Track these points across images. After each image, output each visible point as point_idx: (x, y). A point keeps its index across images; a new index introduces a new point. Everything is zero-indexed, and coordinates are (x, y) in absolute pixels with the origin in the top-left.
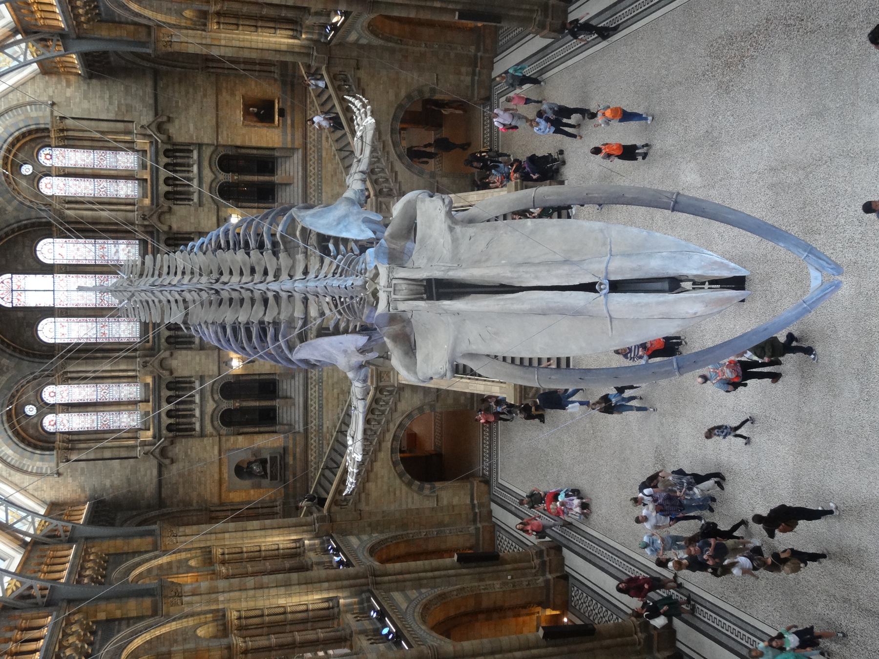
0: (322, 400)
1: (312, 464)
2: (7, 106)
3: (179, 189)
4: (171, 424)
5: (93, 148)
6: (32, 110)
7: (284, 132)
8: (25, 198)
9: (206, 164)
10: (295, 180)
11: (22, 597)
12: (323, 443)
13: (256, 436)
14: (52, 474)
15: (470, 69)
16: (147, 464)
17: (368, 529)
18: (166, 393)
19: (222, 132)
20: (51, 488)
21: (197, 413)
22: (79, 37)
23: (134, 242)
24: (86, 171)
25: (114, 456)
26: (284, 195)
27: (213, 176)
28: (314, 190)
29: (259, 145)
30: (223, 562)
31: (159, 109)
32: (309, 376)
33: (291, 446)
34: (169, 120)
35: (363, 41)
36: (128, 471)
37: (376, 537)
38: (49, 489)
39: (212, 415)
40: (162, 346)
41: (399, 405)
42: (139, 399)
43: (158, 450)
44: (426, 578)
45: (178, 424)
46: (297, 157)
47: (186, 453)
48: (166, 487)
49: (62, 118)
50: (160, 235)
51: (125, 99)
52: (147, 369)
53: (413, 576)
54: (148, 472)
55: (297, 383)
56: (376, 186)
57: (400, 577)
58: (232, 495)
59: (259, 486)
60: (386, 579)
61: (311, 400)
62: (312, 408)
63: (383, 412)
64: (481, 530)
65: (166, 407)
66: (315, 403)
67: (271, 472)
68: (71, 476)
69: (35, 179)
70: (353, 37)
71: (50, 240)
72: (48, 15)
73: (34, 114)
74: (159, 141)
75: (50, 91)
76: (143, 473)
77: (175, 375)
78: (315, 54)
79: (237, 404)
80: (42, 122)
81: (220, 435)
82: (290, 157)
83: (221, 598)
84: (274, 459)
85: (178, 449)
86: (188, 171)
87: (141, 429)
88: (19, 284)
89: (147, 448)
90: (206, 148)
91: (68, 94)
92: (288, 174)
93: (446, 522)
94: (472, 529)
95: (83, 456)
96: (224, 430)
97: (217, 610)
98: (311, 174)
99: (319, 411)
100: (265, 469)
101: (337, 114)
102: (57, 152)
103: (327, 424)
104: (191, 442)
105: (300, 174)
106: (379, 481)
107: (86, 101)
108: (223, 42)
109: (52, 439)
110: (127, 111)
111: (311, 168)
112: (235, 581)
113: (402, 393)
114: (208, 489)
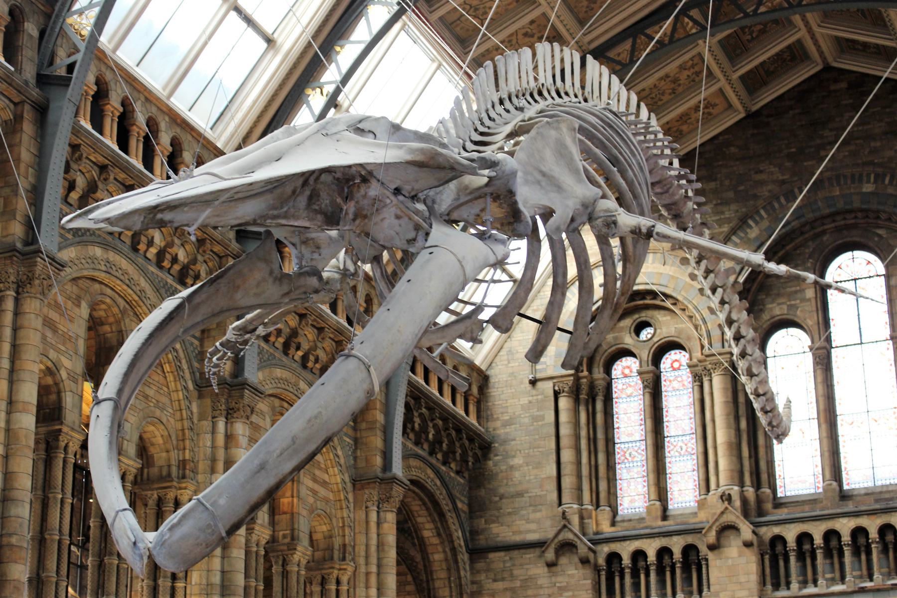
16: (548, 523)
18: (677, 545)
20: (512, 375)
25: (562, 466)
36: (537, 492)
40: (763, 530)
42: (670, 507)
43: (570, 536)
48: (507, 558)
54: (533, 526)
65: (651, 548)
68: (530, 402)
76: (532, 516)
77: (711, 556)
87: (615, 513)
89: (575, 520)
95: (564, 417)
97: (195, 471)
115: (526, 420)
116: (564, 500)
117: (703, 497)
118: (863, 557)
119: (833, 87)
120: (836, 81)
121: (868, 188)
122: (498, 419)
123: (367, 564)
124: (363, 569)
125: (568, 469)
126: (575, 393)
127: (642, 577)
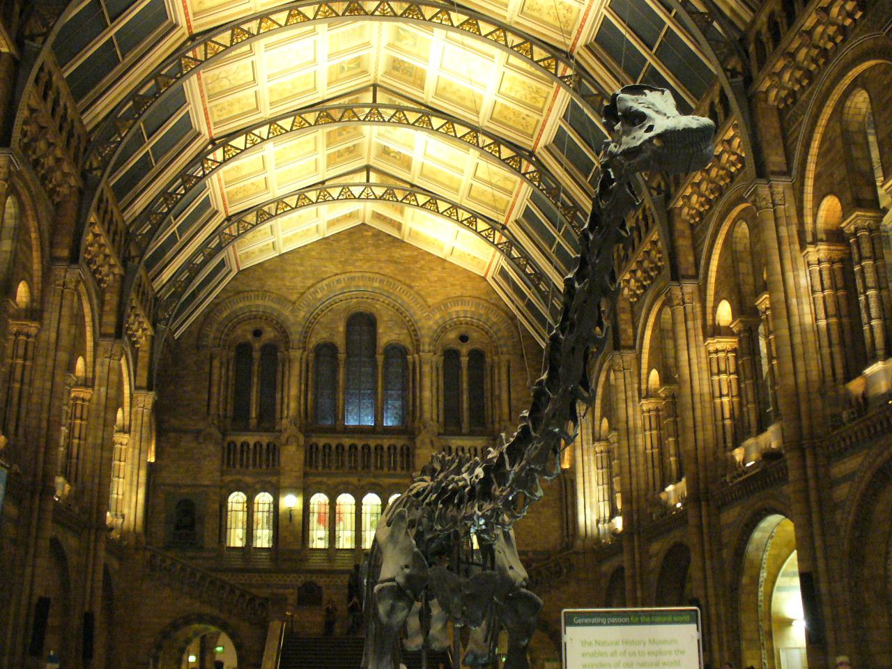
47: (205, 456)
83: (103, 389)
89: (216, 422)
95: (216, 372)
108: (586, 458)
119: (365, 233)
120: (367, 231)
121: (376, 285)
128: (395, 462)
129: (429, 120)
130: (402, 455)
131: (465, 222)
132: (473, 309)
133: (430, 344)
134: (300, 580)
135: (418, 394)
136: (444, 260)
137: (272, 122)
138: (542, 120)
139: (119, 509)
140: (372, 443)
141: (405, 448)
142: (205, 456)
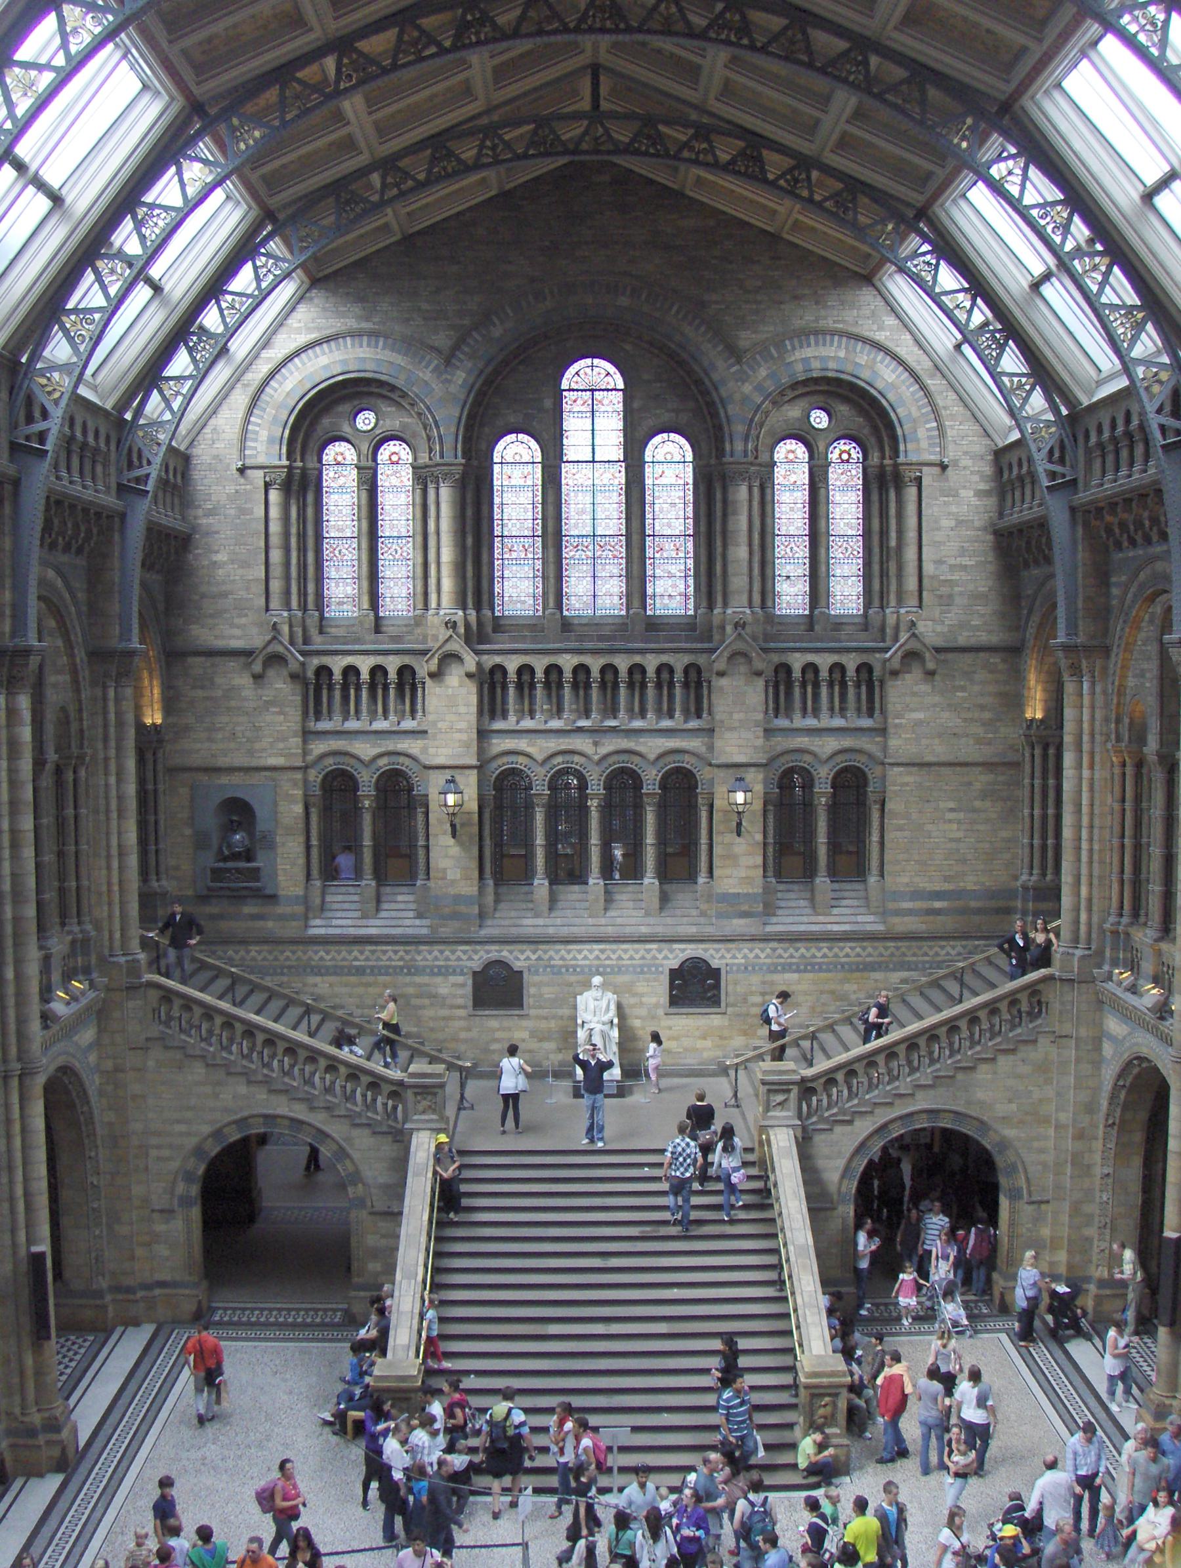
0: (372, 973)
1: (242, 953)
2: (932, 389)
3: (797, 691)
4: (330, 672)
5: (867, 535)
6: (928, 430)
7: (917, 895)
8: (767, 414)
9: (847, 742)
10: (821, 919)
11: (30, 400)
12: (282, 974)
13: (302, 839)
14: (242, 456)
15: (1062, 1270)
16: (254, 631)
17: (109, 1065)
18: (392, 665)
19: (910, 774)
20: (216, 457)
21: (352, 725)
22: (1073, 510)
23: (691, 606)
24: (822, 523)
25: (272, 568)
26: (792, 895)
27: (824, 757)
28: (803, 956)
29: (887, 844)
30: (59, 771)
31: (950, 656)
32: (422, 948)
33: (280, 910)
34: (931, 674)
35: (1108, 1049)
37: (93, 1083)
38: (215, 452)
39: (346, 754)
40: (485, 657)
41: (367, 1131)
43: (281, 649)
44: (11, 1182)
45: (331, 688)
46: (869, 922)
47: (269, 704)
49: (919, 481)
50: (705, 656)
51: (961, 594)
52: (443, 630)
53: (18, 1155)
54: (237, 632)
55: (408, 922)
56: (822, 1080)
57: (17, 1127)
58: (184, 791)
59: (200, 842)
60: (15, 1099)
61: (373, 952)
62: (356, 953)
63: (350, 1098)
64: (98, 1302)
65: (365, 665)
66: (367, 959)
67: (228, 870)
69: (805, 436)
70: (1114, 1025)
71: (689, 456)
72: (1110, 458)
73: (921, 433)
74: (888, 655)
75: (966, 462)
76: (236, 621)
77: (428, 680)
78: (1079, 953)
79: (367, 803)
80: (909, 446)
81: (305, 769)
82: (868, 907)
84: (255, 874)
85: (280, 686)
86: (832, 709)
87: (322, 618)
88: (606, 402)
89: (285, 629)
90: (877, 743)
91: (963, 493)
92: (834, 903)
93: (117, 1227)
94: (104, 1284)
95: (274, 512)
96: (316, 777)
98: (836, 950)
99: (350, 967)
100: (235, 856)
101: (961, 1001)
102: (855, 474)
103: (322, 985)
104: (295, 715)
105: (836, 928)
106: (208, 1089)
107: (953, 523)
108: (1086, 773)
109: (308, 457)
110: (941, 596)
111: (848, 950)
112: (28, 794)
113: (390, 1138)
114: (199, 746)
115: (232, 512)
116: (272, 606)
117: (418, 612)
118: (581, 692)
121: (624, 301)
122: (199, 507)
123: (106, 748)
124: (101, 755)
125: (277, 571)
126: (287, 488)
127: (352, 692)
128: (671, 697)
129: (744, 17)
130: (686, 685)
131: (827, 204)
132: (842, 354)
133: (746, 439)
134: (478, 958)
135: (719, 550)
136: (774, 239)
137: (342, 45)
138: (1037, 51)
139: (85, 909)
140: (622, 663)
141: (693, 676)
142: (269, 704)
